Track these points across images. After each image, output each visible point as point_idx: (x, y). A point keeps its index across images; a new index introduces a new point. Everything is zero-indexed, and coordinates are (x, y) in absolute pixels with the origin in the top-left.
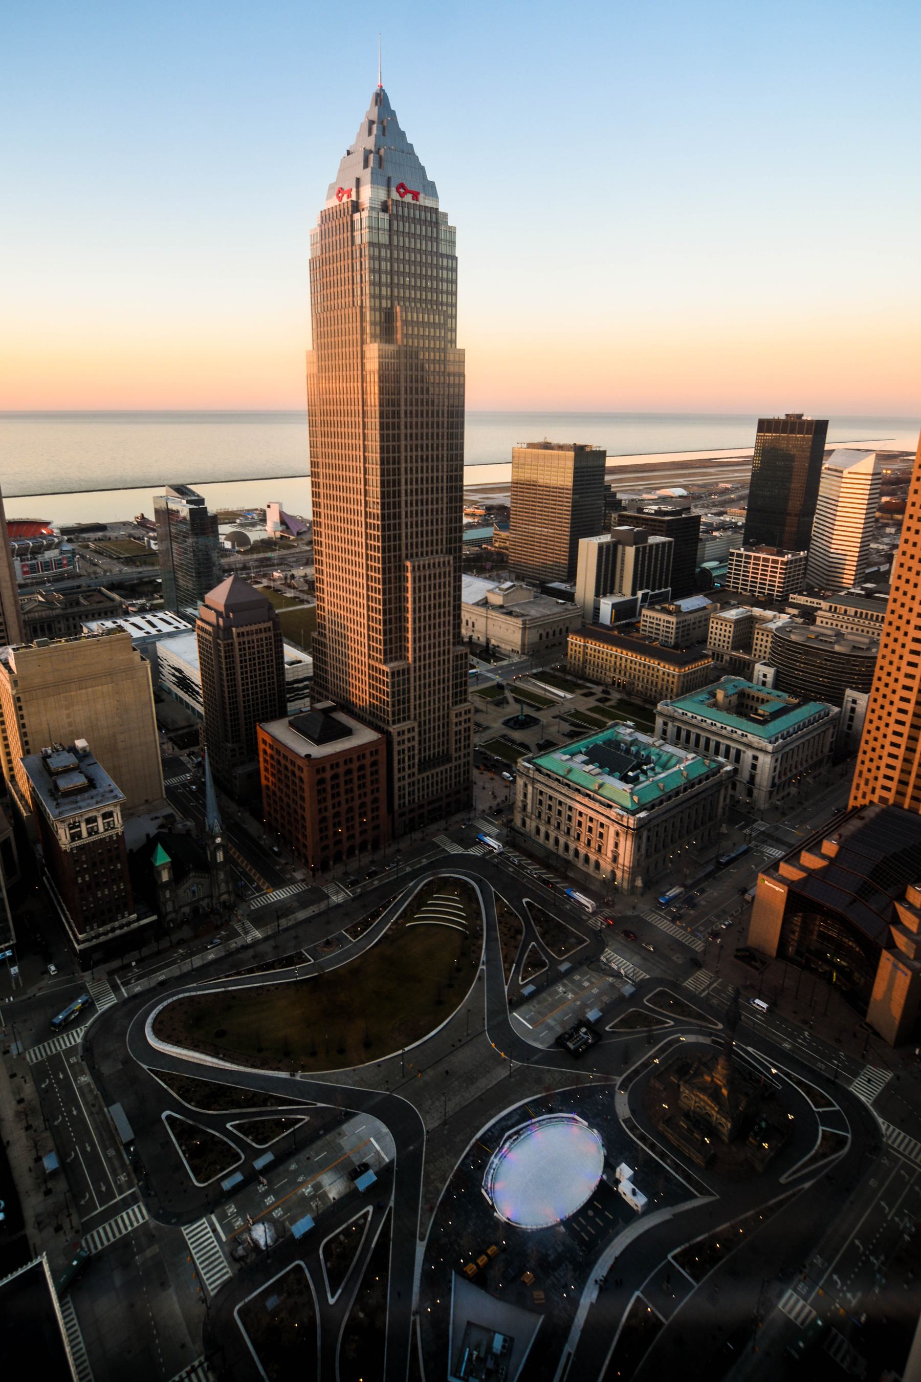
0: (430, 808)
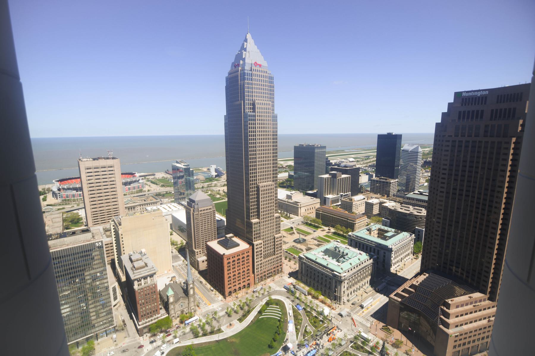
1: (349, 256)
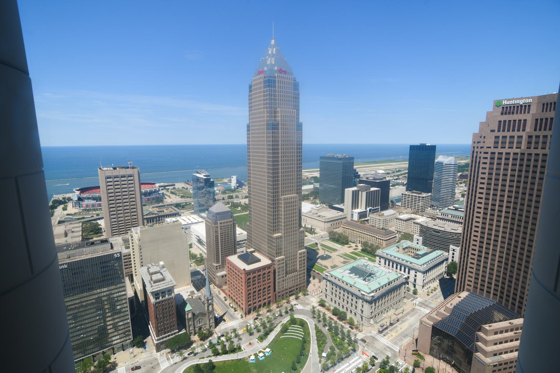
0: (290, 290)
1: (377, 274)
